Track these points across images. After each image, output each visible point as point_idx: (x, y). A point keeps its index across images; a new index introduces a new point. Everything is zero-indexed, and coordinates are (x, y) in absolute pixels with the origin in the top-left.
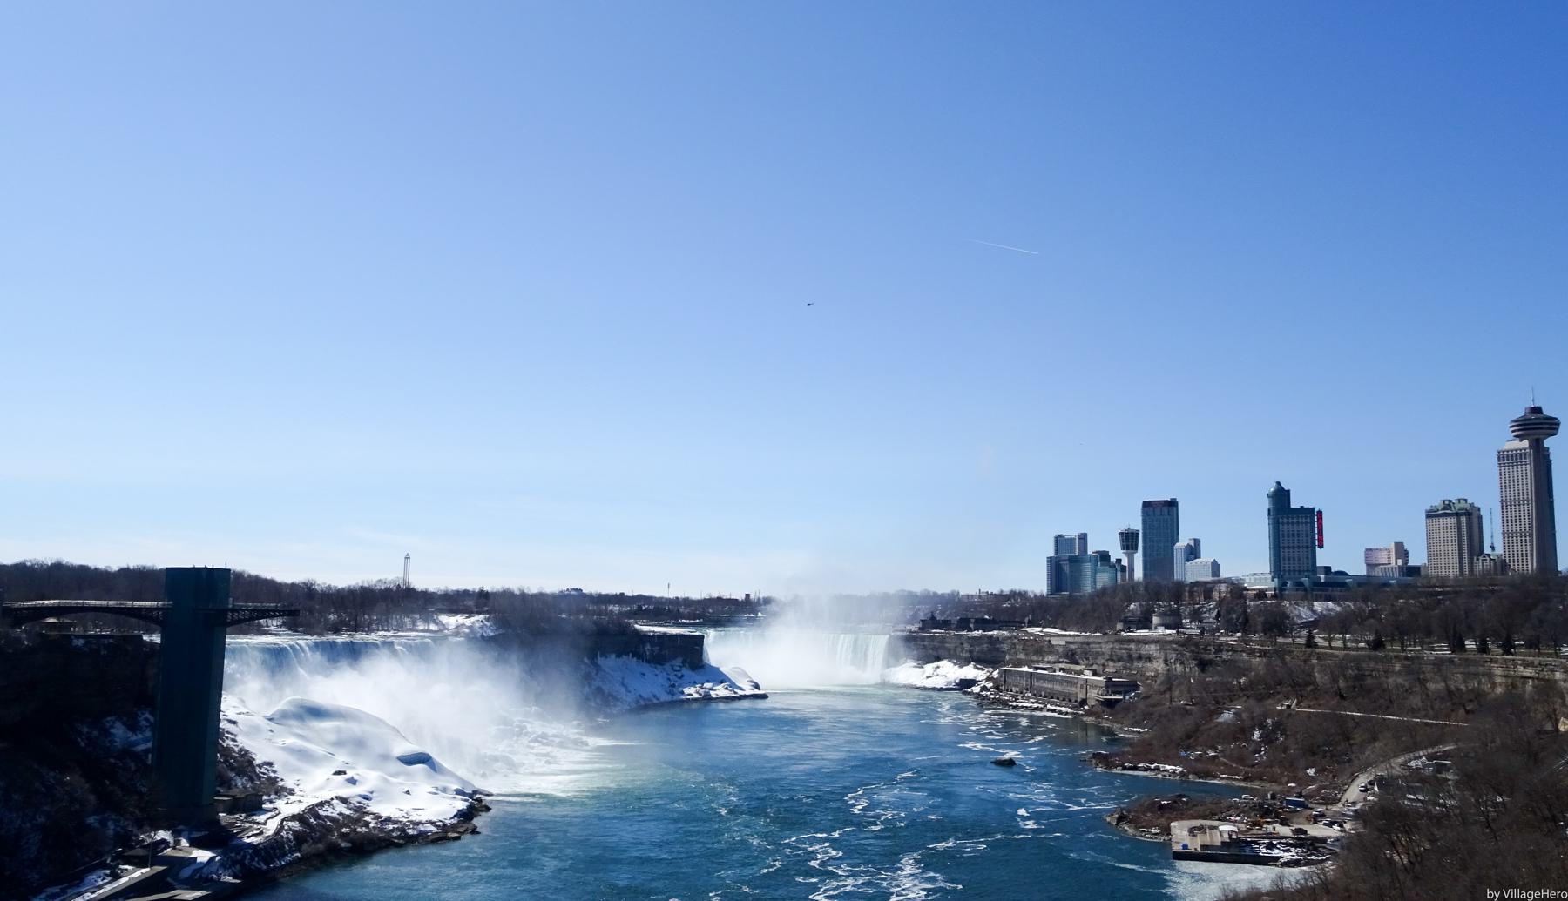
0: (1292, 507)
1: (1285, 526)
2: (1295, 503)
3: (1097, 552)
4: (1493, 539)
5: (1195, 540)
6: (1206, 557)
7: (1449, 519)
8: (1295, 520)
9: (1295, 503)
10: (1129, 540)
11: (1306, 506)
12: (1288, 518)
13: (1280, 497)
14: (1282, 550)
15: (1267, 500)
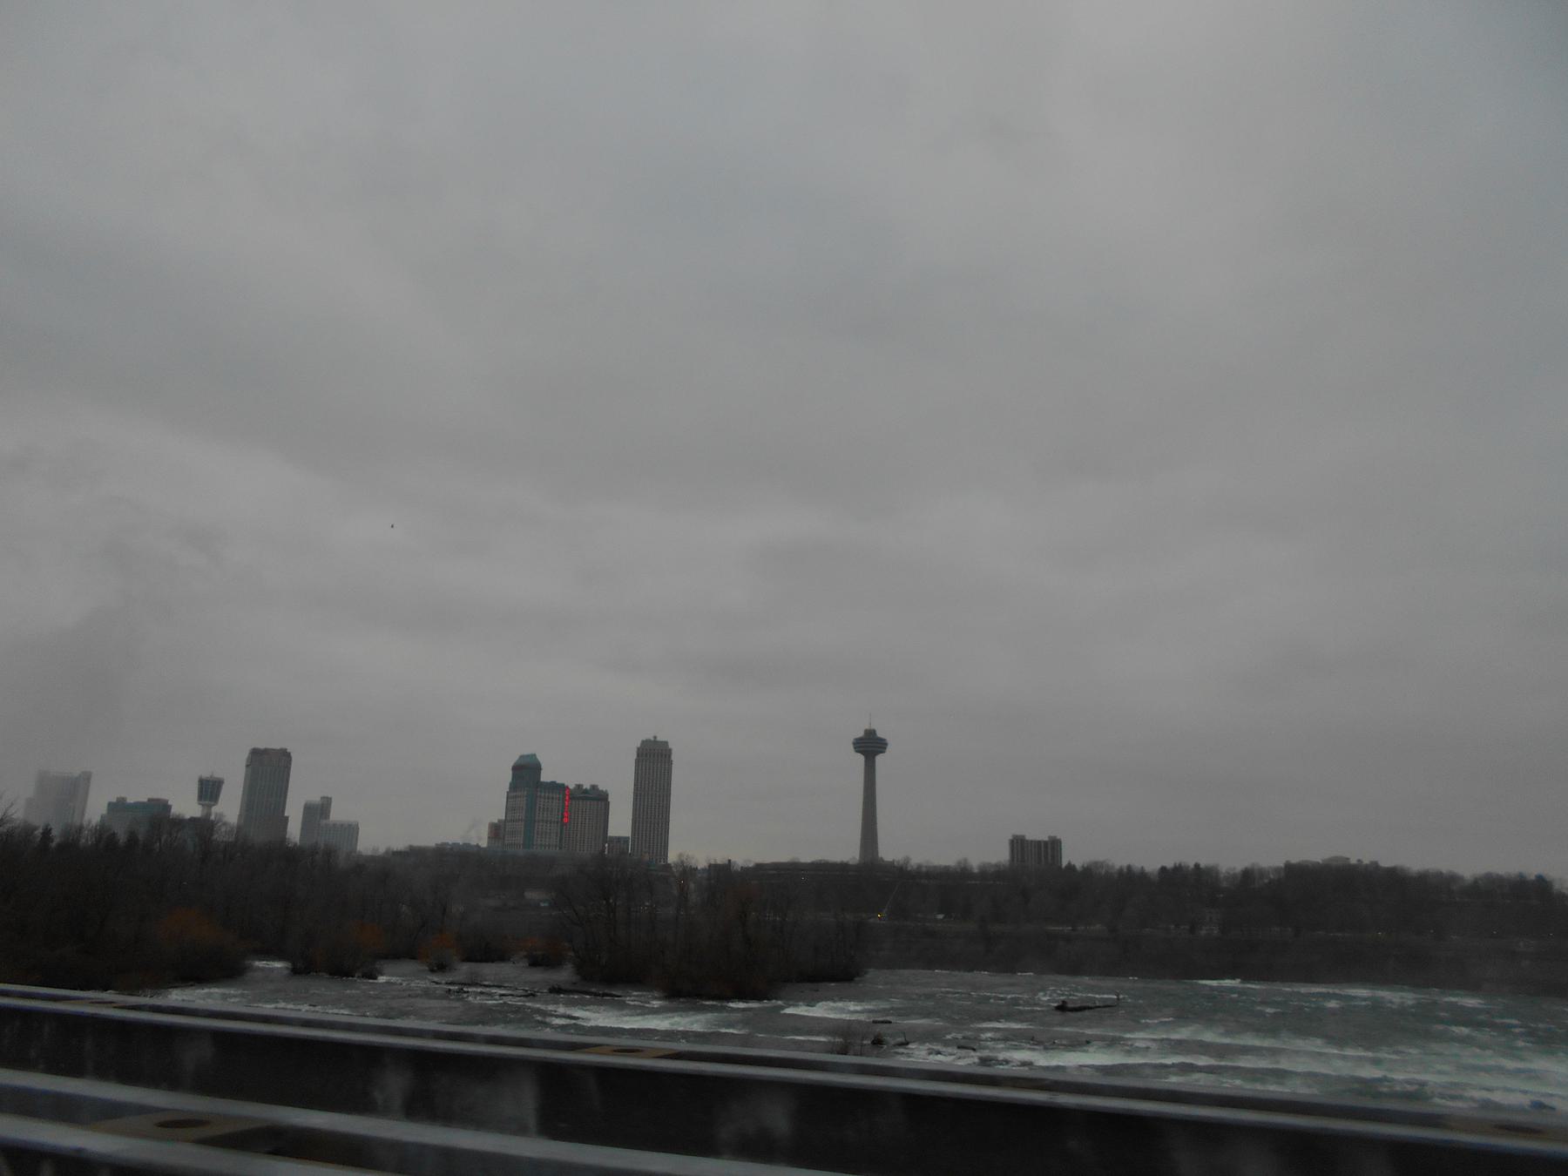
0: (542, 780)
1: (542, 800)
2: (546, 777)
3: (158, 800)
4: (620, 823)
5: (327, 798)
6: (337, 815)
7: (588, 803)
8: (551, 795)
9: (546, 777)
10: (209, 790)
11: (559, 781)
12: (545, 792)
13: (526, 772)
14: (536, 824)
15: (510, 773)
